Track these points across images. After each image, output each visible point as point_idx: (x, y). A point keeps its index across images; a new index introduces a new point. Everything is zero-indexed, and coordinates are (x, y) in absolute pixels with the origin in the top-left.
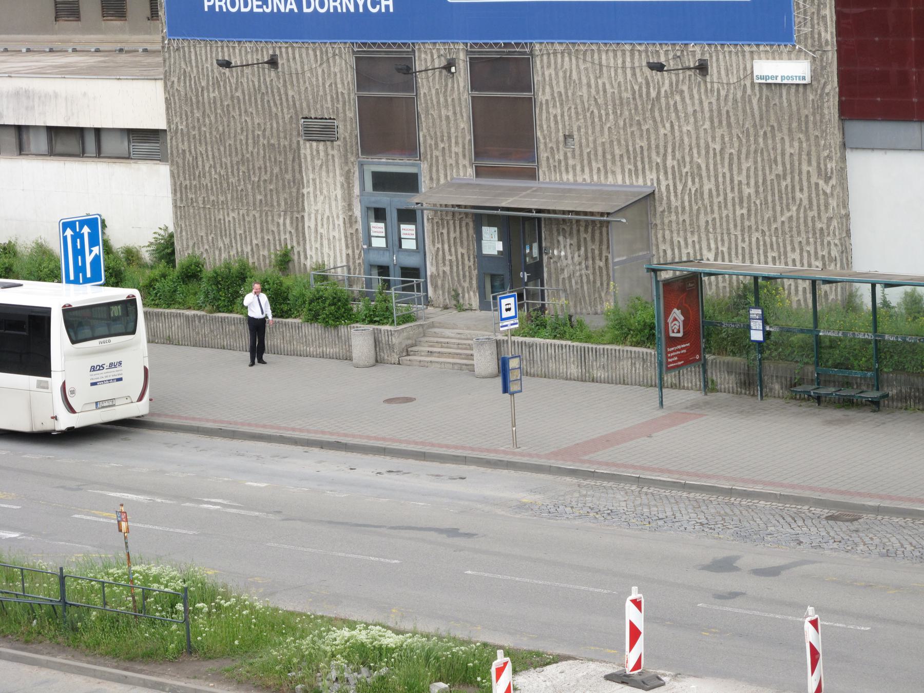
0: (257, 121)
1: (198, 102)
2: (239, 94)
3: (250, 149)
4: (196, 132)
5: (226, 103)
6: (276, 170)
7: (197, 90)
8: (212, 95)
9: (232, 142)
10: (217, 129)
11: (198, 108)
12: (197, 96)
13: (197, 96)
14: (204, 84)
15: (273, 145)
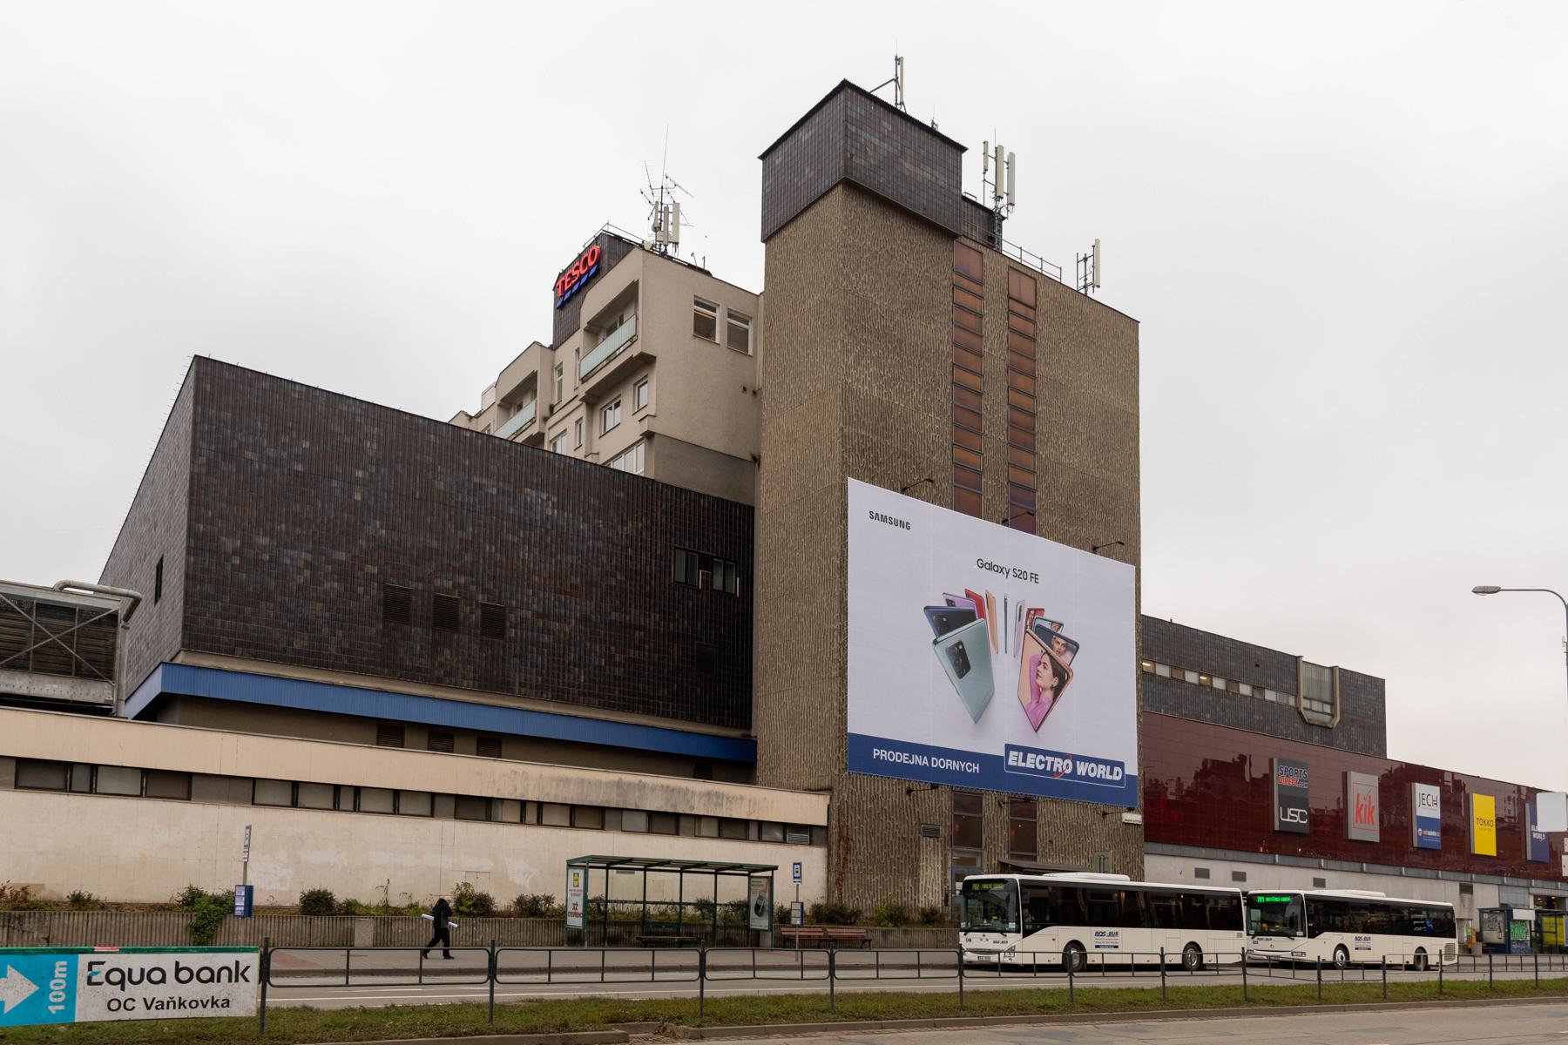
0: (896, 824)
1: (859, 810)
2: (886, 807)
3: (891, 839)
4: (857, 827)
5: (877, 812)
6: (905, 852)
7: (860, 803)
8: (872, 806)
9: (879, 835)
10: (871, 827)
11: (859, 814)
12: (859, 806)
13: (859, 806)
14: (864, 799)
15: (904, 838)
